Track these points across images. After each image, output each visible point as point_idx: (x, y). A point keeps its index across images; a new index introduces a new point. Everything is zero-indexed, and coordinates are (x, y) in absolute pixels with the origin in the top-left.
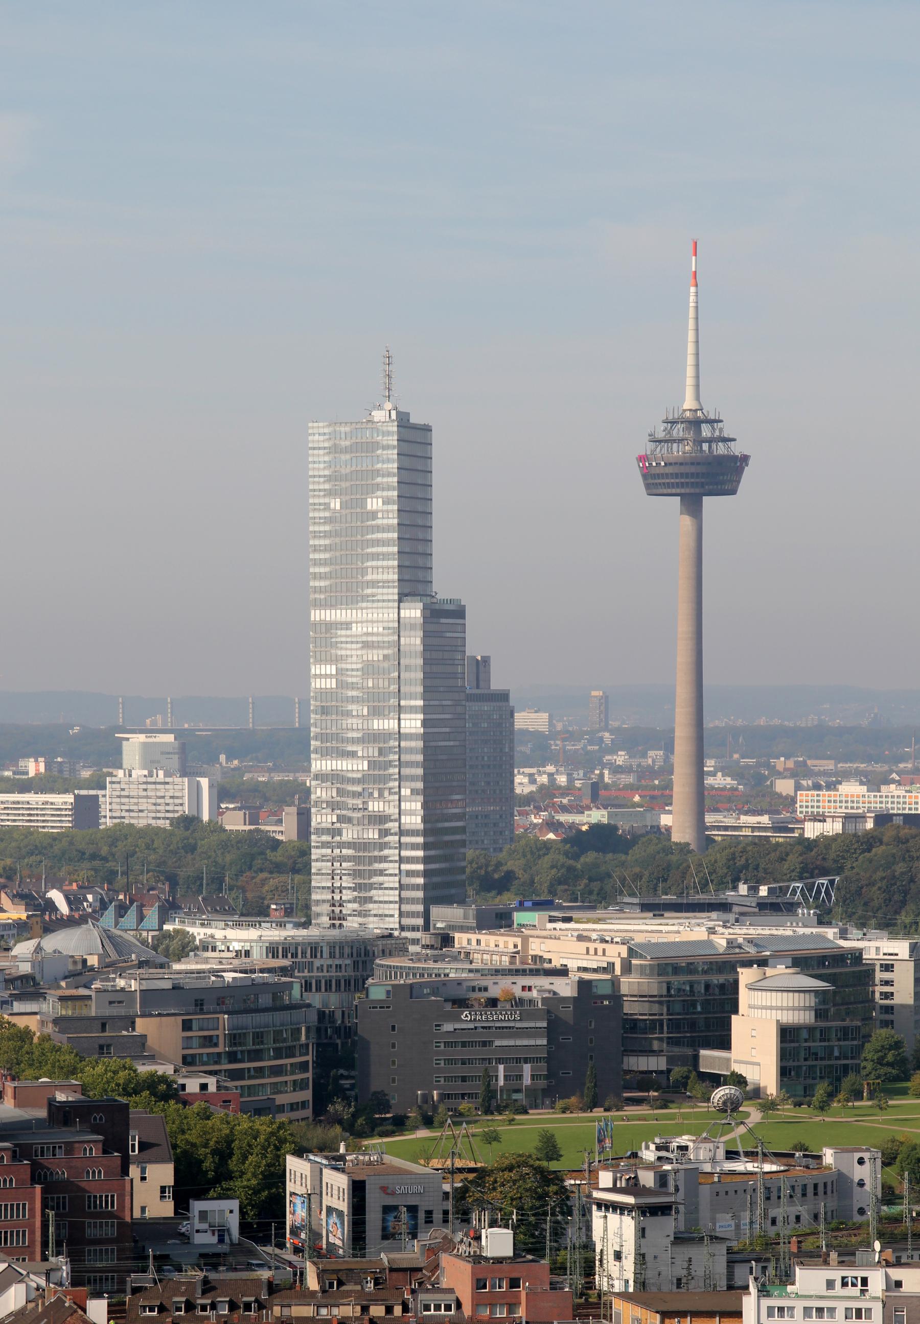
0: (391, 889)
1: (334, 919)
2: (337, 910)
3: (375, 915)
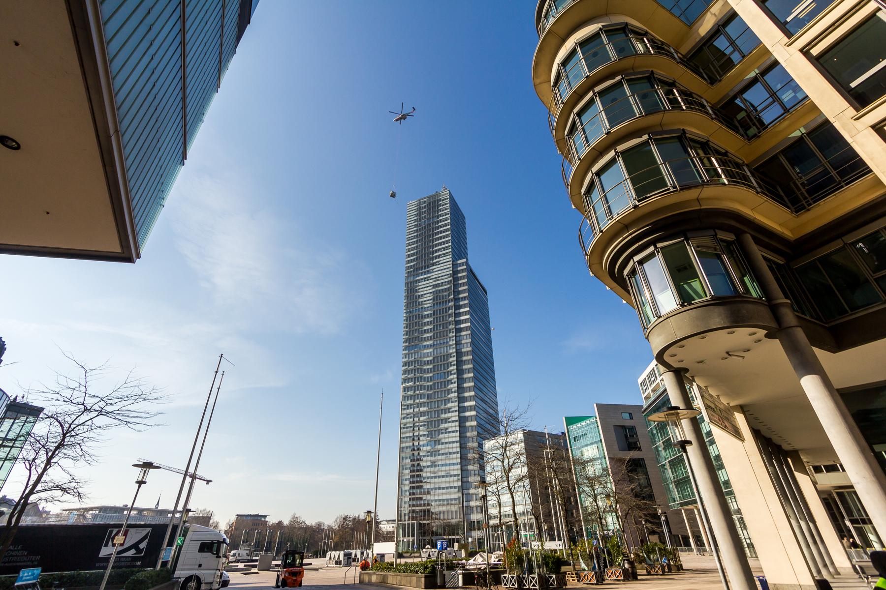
0: (453, 432)
1: (414, 460)
2: (416, 453)
3: (443, 454)
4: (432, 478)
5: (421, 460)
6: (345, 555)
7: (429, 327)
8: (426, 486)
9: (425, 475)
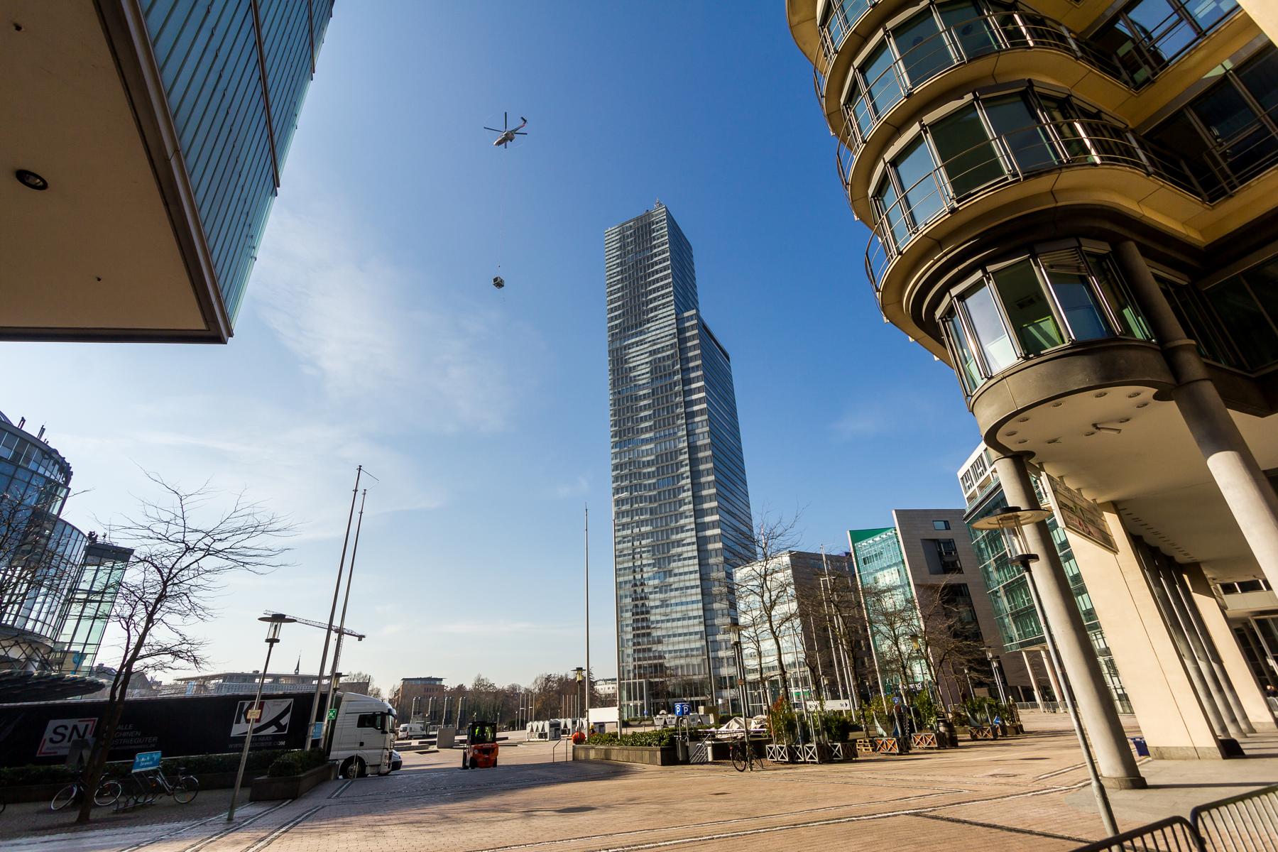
0: (690, 558)
1: (636, 599)
3: (676, 589)
4: (663, 621)
5: (646, 598)
6: (551, 726)
7: (647, 413)
8: (656, 633)
9: (653, 618)
